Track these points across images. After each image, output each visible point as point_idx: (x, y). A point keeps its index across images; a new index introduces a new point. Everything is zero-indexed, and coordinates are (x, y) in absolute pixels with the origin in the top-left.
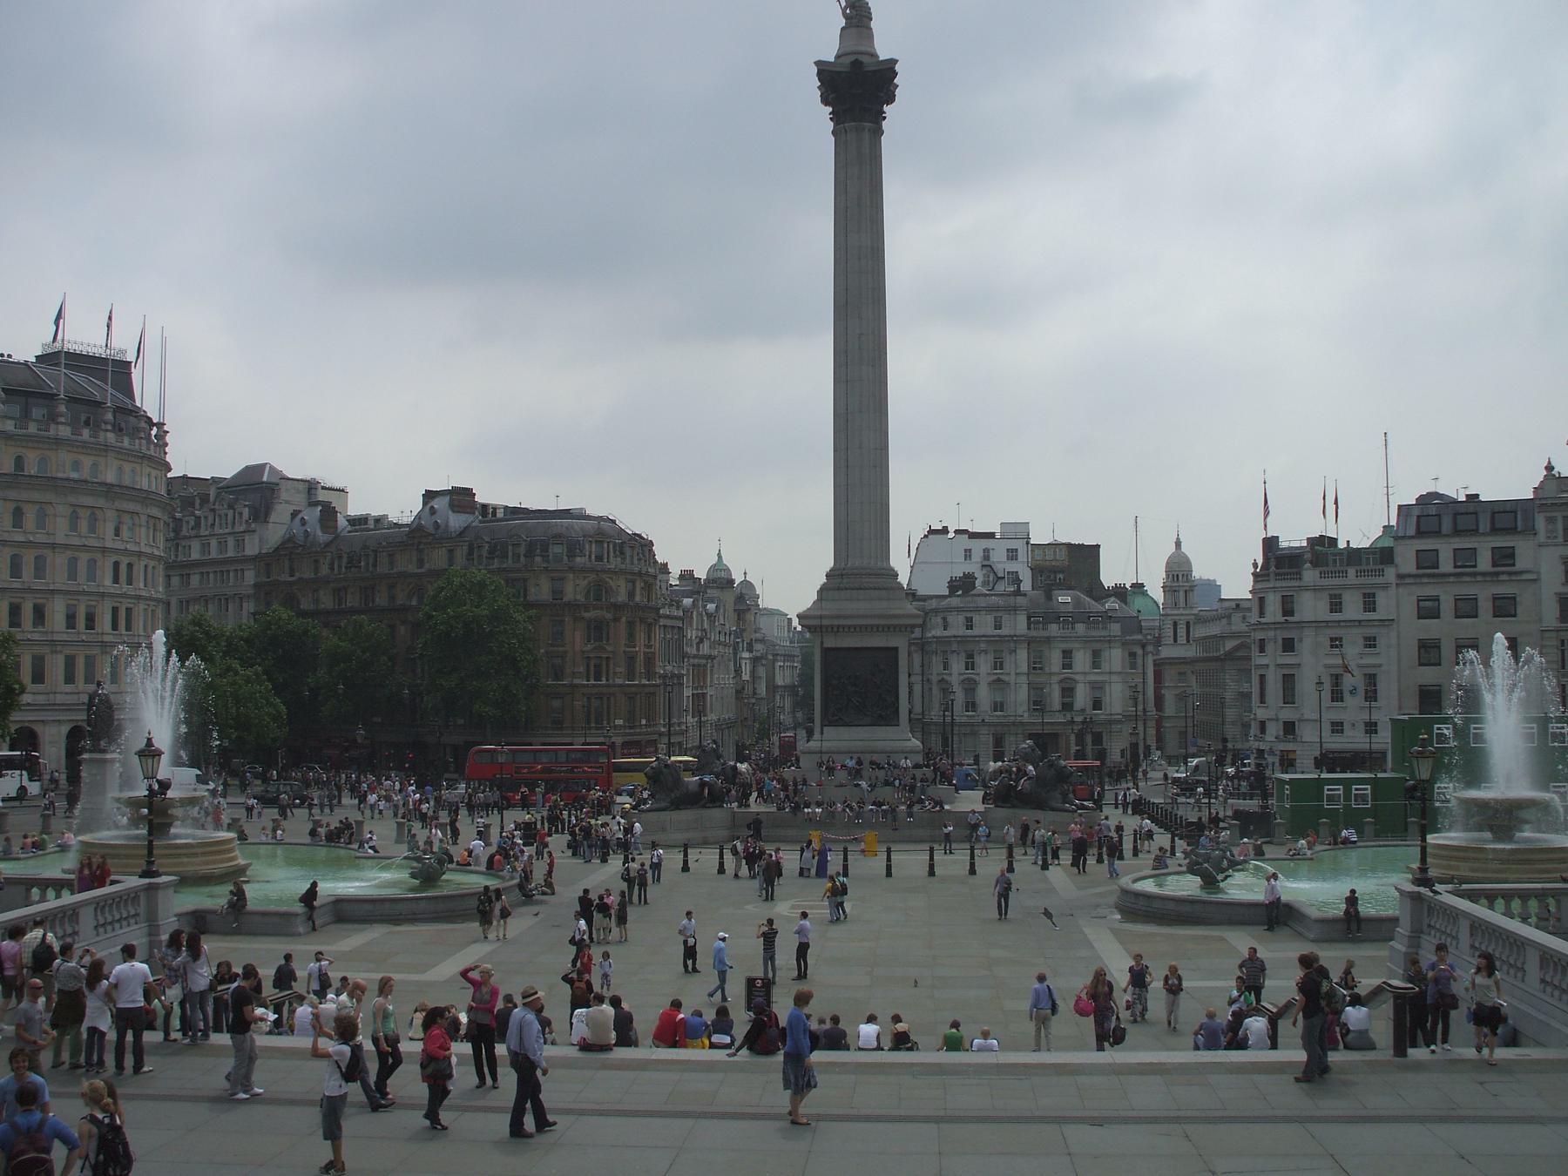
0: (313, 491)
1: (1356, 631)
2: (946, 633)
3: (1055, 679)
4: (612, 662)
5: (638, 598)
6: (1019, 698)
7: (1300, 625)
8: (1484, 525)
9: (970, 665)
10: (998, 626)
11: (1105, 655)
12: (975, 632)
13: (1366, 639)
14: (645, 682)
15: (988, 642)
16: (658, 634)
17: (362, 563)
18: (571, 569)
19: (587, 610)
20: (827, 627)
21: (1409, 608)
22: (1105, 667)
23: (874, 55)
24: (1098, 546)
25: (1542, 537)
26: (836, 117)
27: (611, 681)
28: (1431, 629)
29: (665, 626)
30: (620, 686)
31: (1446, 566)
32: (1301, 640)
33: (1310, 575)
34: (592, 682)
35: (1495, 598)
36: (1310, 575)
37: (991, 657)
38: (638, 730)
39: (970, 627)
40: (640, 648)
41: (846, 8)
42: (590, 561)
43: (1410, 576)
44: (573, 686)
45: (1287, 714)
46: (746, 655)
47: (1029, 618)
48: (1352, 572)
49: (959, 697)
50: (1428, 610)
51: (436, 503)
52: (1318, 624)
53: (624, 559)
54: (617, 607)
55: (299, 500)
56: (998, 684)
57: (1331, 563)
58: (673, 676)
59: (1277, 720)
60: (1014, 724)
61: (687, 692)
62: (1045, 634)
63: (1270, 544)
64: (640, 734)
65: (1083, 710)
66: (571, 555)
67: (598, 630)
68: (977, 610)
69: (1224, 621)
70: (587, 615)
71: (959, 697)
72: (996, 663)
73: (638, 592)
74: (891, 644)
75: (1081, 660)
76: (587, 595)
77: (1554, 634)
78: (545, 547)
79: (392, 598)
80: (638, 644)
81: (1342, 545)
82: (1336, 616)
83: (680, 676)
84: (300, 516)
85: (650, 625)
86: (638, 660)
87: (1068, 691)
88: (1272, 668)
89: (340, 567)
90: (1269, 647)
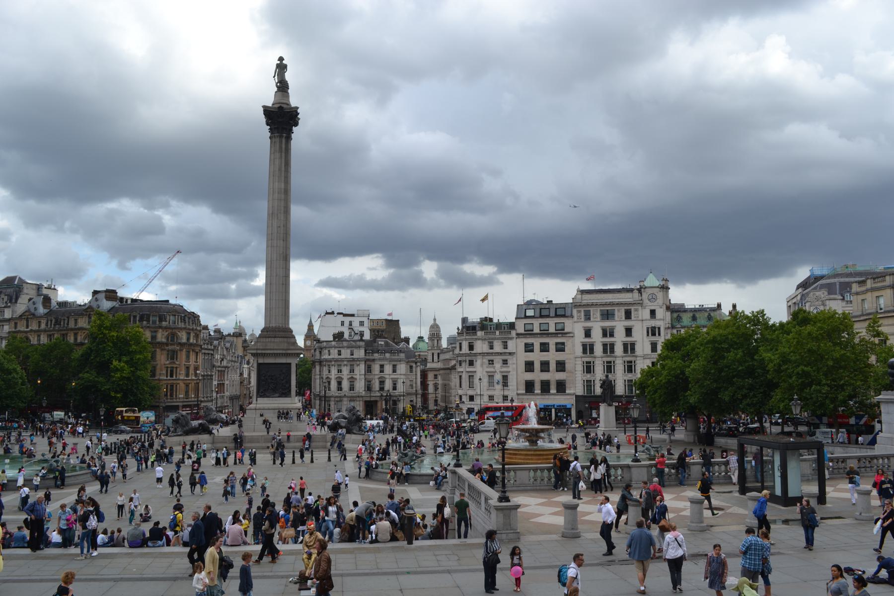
0: (40, 289)
1: (499, 357)
2: (330, 357)
3: (377, 377)
4: (178, 369)
5: (191, 341)
6: (360, 386)
7: (476, 355)
8: (552, 314)
9: (340, 371)
10: (352, 354)
11: (398, 367)
12: (342, 356)
13: (503, 360)
14: (194, 378)
15: (348, 361)
16: (201, 357)
17: (62, 323)
18: (160, 327)
19: (167, 344)
20: (260, 354)
21: (522, 347)
22: (398, 372)
23: (289, 104)
24: (398, 321)
25: (575, 319)
26: (271, 130)
27: (178, 378)
28: (530, 356)
29: (205, 353)
30: (182, 380)
31: (536, 330)
32: (476, 361)
33: (480, 334)
34: (169, 378)
35: (557, 344)
36: (480, 334)
37: (349, 368)
38: (190, 400)
39: (340, 354)
40: (192, 363)
41: (278, 83)
42: (169, 323)
43: (521, 334)
44: (159, 380)
45: (471, 392)
46: (246, 366)
47: (365, 351)
48: (497, 333)
49: (334, 385)
50: (529, 348)
51: (98, 296)
52: (483, 354)
53: (185, 323)
54: (182, 345)
55: (32, 293)
56: (352, 380)
57: (489, 329)
58: (207, 375)
59: (466, 395)
60: (358, 397)
61: (215, 383)
62: (371, 357)
63: (464, 320)
64: (191, 401)
65: (388, 391)
66: (161, 320)
67: (173, 355)
68: (343, 347)
69: (451, 353)
70: (167, 348)
71: (334, 385)
72: (351, 370)
73: (192, 337)
74: (288, 362)
75: (388, 369)
76: (168, 339)
77: (580, 359)
78: (148, 316)
79: (76, 339)
81: (495, 321)
82: (491, 351)
83: (212, 376)
84: (33, 300)
85: (197, 353)
87: (382, 383)
88: (464, 373)
89: (51, 325)
90: (463, 364)
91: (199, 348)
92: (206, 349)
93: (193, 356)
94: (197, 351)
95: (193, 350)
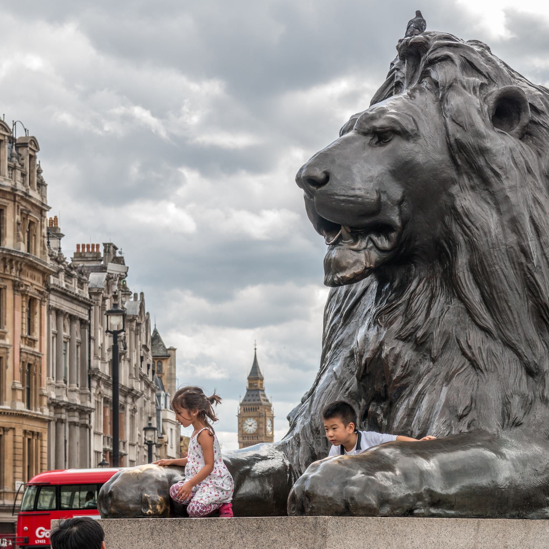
14: (21, 406)
29: (58, 312)
58: (70, 408)
80: (10, 334)
86: (10, 363)
91: (38, 284)
92: (64, 294)
93: (18, 314)
94: (32, 291)
95: (16, 286)
